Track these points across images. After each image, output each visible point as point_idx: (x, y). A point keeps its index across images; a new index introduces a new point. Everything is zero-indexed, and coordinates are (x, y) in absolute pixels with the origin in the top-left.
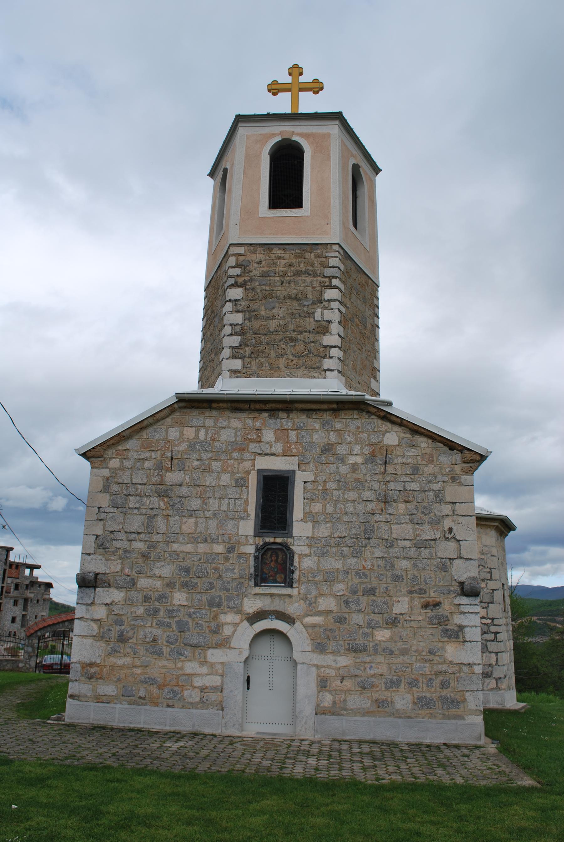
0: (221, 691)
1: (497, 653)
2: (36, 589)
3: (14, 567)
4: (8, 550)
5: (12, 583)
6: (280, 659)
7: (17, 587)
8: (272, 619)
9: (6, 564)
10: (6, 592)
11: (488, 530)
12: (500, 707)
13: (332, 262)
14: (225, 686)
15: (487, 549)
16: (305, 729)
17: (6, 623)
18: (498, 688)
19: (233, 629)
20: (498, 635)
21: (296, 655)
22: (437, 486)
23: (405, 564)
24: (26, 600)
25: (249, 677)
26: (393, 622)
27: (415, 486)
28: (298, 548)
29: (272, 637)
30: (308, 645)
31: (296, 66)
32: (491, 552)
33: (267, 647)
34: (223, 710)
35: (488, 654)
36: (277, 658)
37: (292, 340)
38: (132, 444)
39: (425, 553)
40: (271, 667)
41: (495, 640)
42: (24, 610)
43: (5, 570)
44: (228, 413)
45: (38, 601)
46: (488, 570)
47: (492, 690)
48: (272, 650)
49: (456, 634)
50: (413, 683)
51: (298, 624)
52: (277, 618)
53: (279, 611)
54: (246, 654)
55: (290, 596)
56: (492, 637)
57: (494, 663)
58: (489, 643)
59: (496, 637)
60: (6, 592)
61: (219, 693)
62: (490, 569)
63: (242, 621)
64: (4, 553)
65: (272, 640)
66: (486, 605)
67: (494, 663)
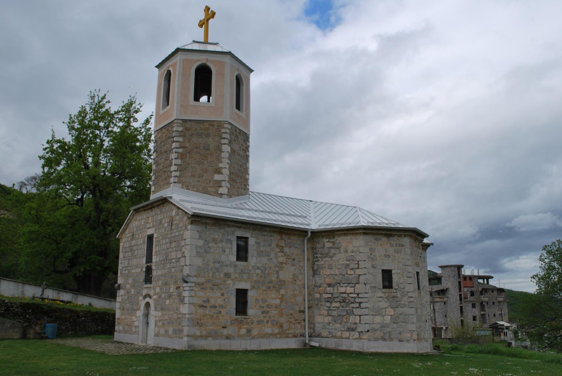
1: (360, 316)
2: (490, 294)
3: (468, 279)
4: (459, 267)
5: (468, 291)
7: (472, 294)
9: (459, 277)
10: (465, 298)
11: (358, 236)
12: (361, 350)
13: (175, 129)
15: (356, 248)
17: (469, 321)
18: (360, 338)
20: (361, 304)
22: (182, 233)
23: (173, 270)
24: (482, 303)
26: (170, 296)
27: (177, 234)
28: (153, 268)
31: (207, 7)
32: (358, 251)
35: (354, 316)
37: (165, 172)
38: (127, 232)
39: (178, 263)
41: (359, 307)
42: (483, 311)
43: (460, 283)
44: (144, 213)
45: (493, 303)
46: (357, 262)
47: (355, 339)
49: (182, 301)
50: (173, 323)
55: (151, 287)
56: (357, 305)
57: (358, 322)
58: (354, 310)
59: (360, 305)
60: (465, 298)
62: (358, 261)
64: (456, 269)
66: (354, 285)
67: (358, 322)
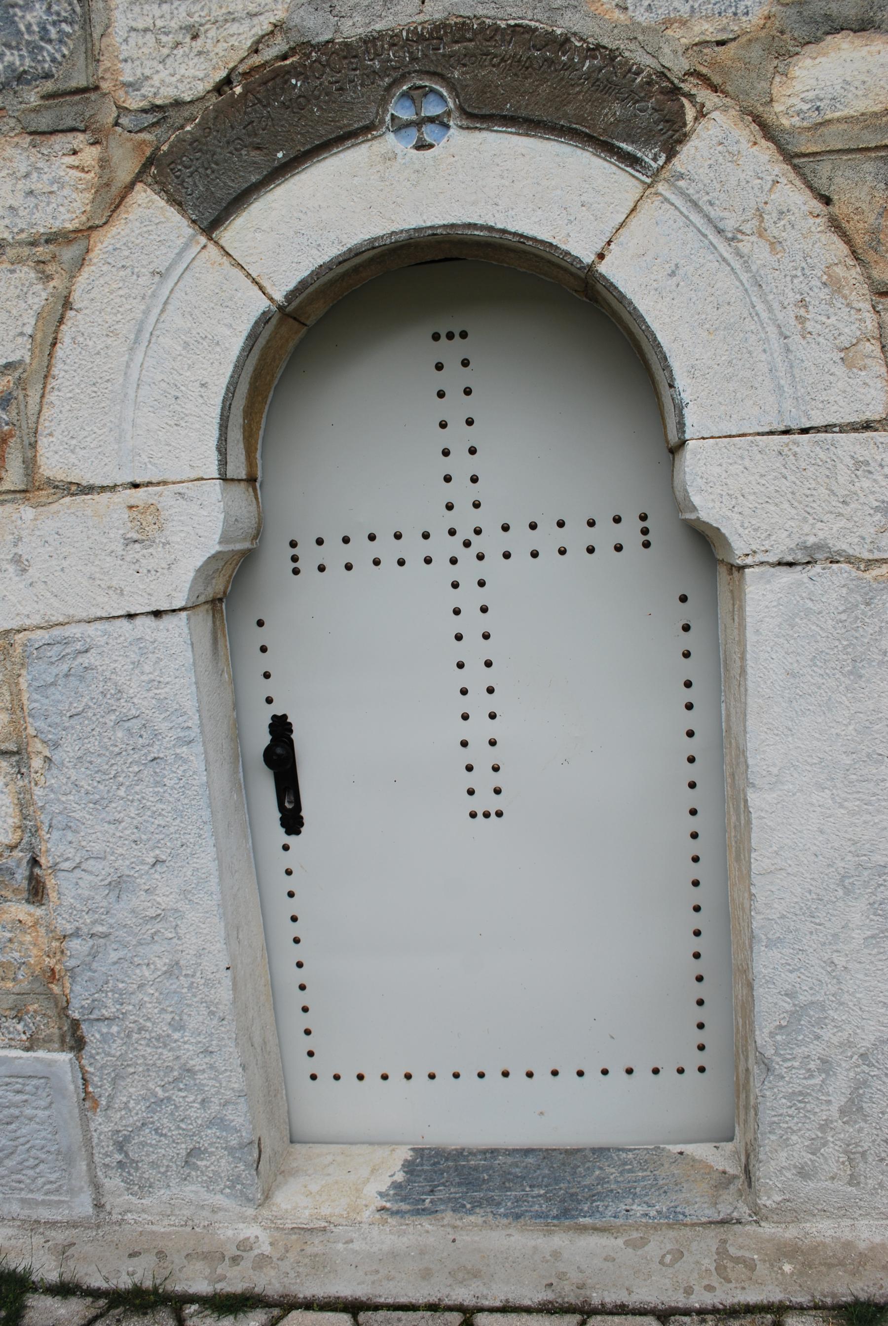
0: (36, 891)
6: (548, 538)
8: (421, 131)
14: (54, 848)
16: (853, 1156)
19: (40, 296)
21: (716, 483)
25: (281, 728)
29: (450, 352)
30: (848, 355)
33: (394, 439)
34: (75, 1041)
36: (520, 541)
40: (472, 623)
48: (461, 465)
51: (717, 146)
52: (483, 113)
53: (490, 33)
54: (201, 525)
61: (20, 910)
63: (112, 201)
65: (454, 378)
